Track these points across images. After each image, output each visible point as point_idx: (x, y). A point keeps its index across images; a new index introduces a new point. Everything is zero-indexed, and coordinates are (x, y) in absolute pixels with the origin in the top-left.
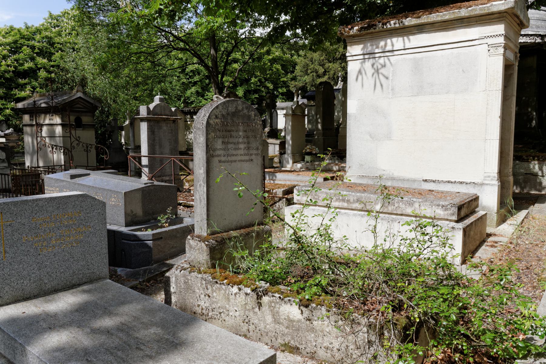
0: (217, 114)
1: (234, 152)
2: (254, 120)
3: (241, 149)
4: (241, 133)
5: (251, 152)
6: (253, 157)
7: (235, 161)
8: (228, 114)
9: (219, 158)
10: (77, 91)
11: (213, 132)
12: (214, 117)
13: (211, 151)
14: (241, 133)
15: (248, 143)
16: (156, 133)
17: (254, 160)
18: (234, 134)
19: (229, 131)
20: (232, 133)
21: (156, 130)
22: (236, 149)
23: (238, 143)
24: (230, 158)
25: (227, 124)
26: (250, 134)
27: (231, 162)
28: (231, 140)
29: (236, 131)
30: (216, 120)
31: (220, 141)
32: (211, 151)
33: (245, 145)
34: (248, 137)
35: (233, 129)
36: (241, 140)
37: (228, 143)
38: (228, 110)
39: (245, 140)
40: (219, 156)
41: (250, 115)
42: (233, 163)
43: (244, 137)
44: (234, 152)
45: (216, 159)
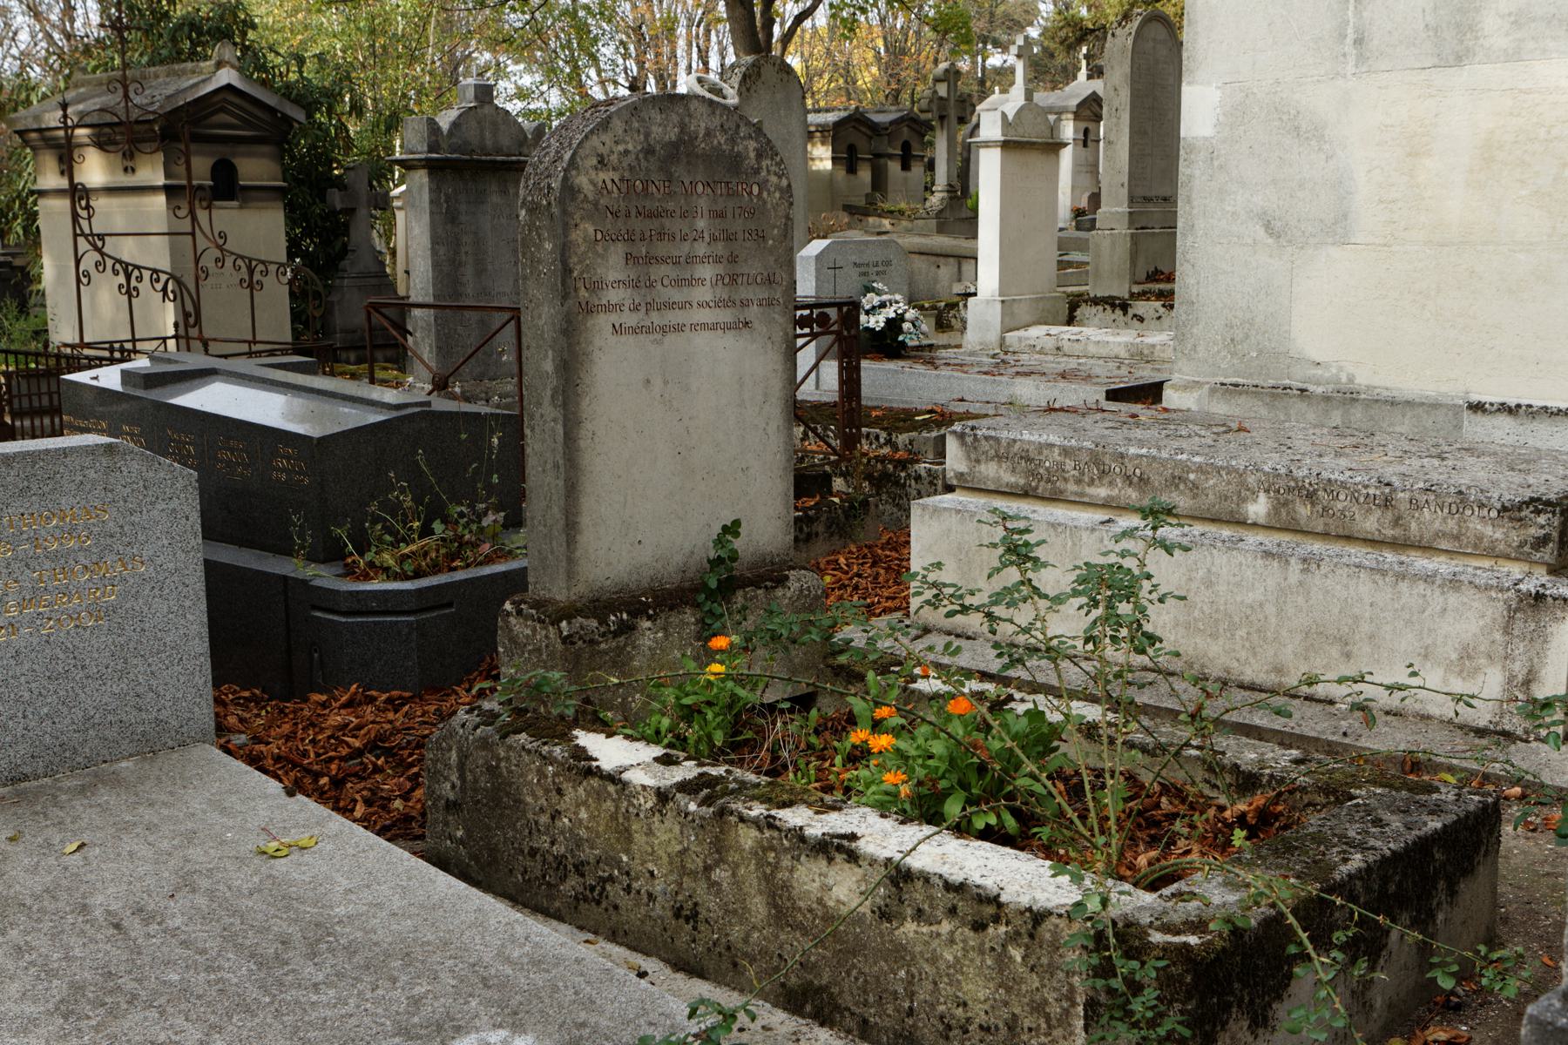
0: (601, 149)
1: (676, 295)
2: (757, 171)
3: (702, 281)
4: (701, 224)
5: (745, 293)
6: (753, 312)
7: (679, 328)
8: (649, 151)
9: (614, 318)
10: (219, 65)
11: (589, 217)
12: (594, 162)
13: (583, 293)
14: (701, 224)
15: (733, 259)
16: (463, 218)
17: (756, 324)
18: (674, 225)
19: (651, 215)
20: (667, 222)
21: (463, 207)
22: (679, 283)
23: (691, 260)
24: (656, 318)
25: (645, 189)
26: (738, 226)
27: (664, 330)
28: (662, 249)
29: (683, 216)
30: (602, 176)
31: (617, 253)
32: (583, 293)
33: (720, 269)
34: (730, 238)
35: (671, 206)
36: (701, 249)
37: (651, 260)
38: (647, 135)
39: (720, 249)
40: (610, 308)
41: (739, 154)
42: (671, 338)
43: (714, 239)
44: (676, 295)
45: (603, 321)
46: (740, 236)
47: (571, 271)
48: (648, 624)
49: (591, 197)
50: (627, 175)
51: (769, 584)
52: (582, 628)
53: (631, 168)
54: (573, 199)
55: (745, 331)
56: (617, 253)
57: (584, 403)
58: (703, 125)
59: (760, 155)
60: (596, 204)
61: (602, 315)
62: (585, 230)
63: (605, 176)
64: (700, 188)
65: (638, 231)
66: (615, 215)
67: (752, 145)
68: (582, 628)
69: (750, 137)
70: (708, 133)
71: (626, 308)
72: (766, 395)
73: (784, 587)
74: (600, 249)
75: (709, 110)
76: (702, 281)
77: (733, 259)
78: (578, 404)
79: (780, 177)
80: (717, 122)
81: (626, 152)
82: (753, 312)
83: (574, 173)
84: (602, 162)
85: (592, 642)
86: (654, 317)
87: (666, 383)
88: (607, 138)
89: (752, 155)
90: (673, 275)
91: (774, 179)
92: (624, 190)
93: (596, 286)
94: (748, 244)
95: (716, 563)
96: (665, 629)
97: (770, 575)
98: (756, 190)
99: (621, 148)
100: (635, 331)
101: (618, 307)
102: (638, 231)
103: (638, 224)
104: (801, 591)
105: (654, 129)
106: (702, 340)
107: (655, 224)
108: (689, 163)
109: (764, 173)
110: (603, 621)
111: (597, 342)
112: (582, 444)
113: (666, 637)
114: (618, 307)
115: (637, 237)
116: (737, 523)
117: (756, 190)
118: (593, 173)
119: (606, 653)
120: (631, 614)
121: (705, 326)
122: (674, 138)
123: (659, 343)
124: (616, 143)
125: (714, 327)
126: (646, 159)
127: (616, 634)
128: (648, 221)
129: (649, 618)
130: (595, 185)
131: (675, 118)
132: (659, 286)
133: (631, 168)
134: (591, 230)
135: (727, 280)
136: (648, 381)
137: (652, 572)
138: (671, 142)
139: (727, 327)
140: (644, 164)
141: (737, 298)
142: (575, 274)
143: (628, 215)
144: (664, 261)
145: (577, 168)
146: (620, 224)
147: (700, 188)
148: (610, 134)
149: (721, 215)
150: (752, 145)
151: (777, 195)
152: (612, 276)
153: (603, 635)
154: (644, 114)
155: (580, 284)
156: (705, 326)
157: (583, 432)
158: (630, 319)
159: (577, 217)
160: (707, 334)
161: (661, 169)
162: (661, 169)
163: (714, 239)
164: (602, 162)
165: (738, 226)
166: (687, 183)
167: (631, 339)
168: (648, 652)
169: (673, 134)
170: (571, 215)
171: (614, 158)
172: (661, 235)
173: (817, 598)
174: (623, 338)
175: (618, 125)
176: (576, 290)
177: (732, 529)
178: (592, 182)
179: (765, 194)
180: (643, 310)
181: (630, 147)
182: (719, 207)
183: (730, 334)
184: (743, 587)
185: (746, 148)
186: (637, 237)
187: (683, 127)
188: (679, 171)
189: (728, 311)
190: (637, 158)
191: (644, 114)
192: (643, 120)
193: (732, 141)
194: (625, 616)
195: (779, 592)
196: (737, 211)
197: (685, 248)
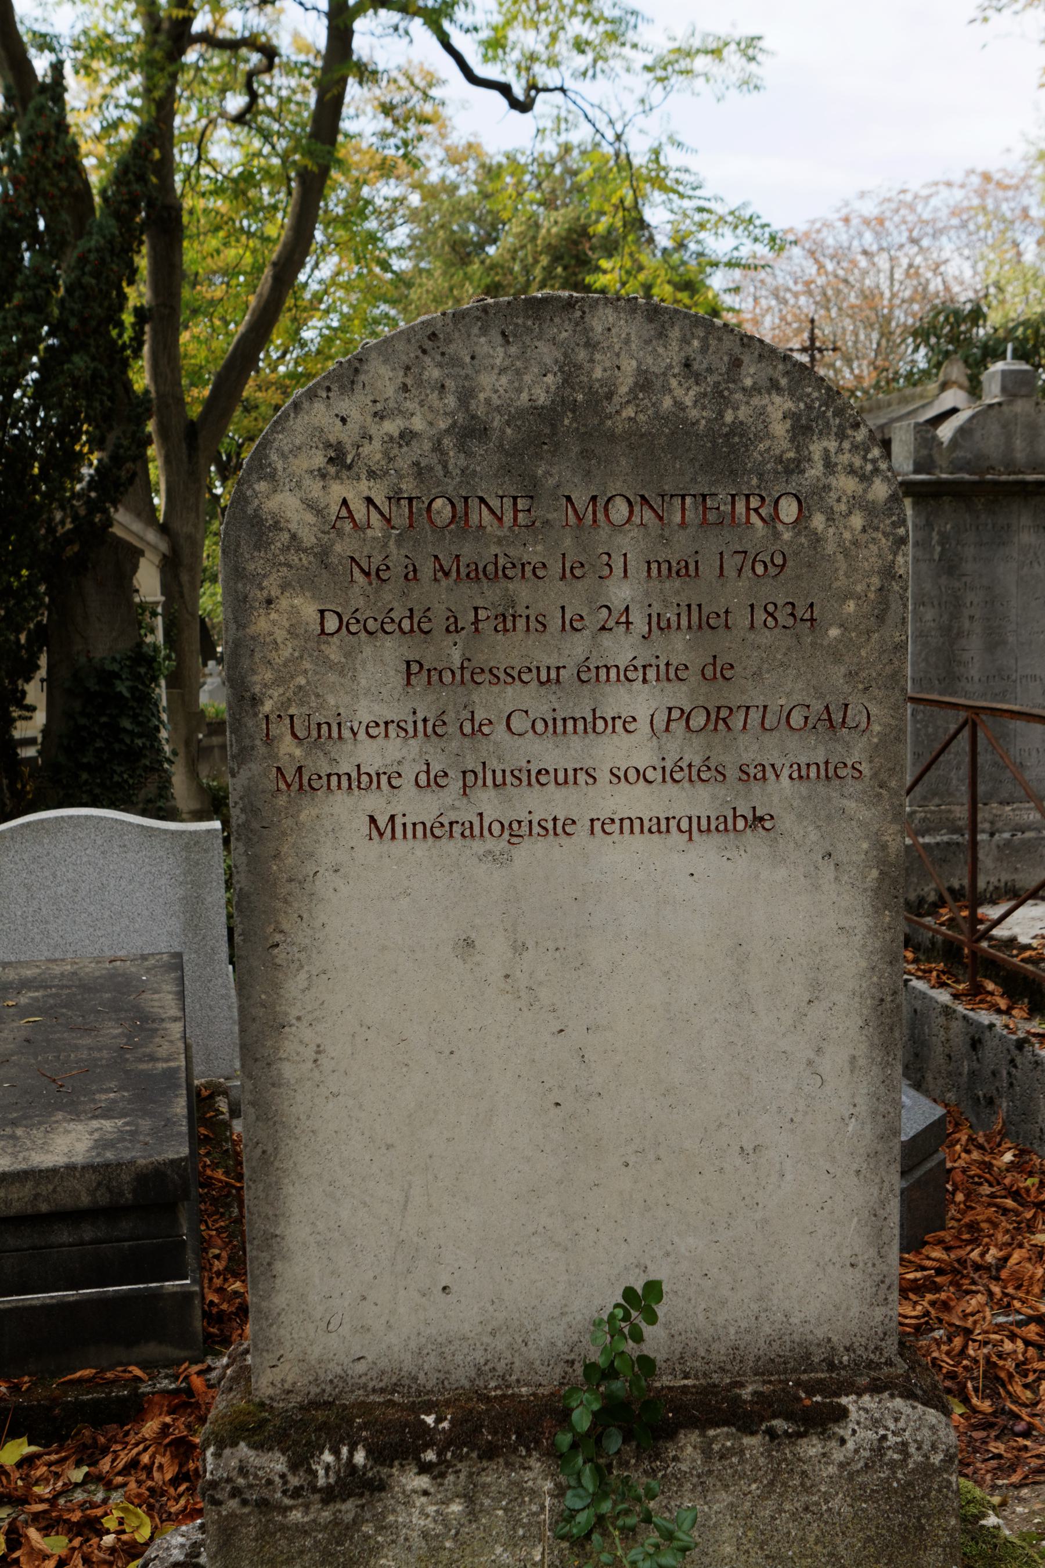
0: (336, 432)
1: (549, 754)
2: (794, 467)
3: (628, 724)
4: (621, 593)
5: (749, 750)
6: (779, 794)
7: (558, 828)
8: (471, 431)
9: (375, 803)
11: (306, 583)
12: (319, 460)
13: (288, 748)
14: (621, 593)
15: (718, 672)
16: (969, 567)
17: (787, 822)
18: (547, 597)
19: (476, 574)
20: (523, 592)
22: (556, 726)
23: (591, 674)
24: (489, 803)
25: (460, 518)
26: (735, 594)
27: (513, 831)
28: (507, 650)
29: (570, 574)
30: (338, 490)
31: (380, 663)
32: (288, 748)
33: (679, 695)
34: (706, 623)
35: (533, 552)
36: (621, 649)
37: (471, 674)
38: (466, 396)
39: (678, 647)
40: (359, 781)
41: (738, 428)
42: (531, 852)
43: (659, 625)
44: (549, 754)
45: (345, 812)
46: (741, 619)
47: (256, 701)
48: (423, 1482)
49: (308, 538)
50: (408, 487)
51: (779, 1424)
52: (243, 1471)
53: (420, 471)
54: (261, 543)
55: (753, 839)
56: (380, 663)
57: (294, 985)
58: (629, 366)
59: (801, 429)
60: (323, 555)
61: (340, 796)
62: (294, 611)
63: (352, 490)
64: (620, 510)
65: (439, 613)
66: (376, 575)
67: (779, 405)
68: (243, 1471)
69: (774, 386)
70: (645, 383)
71: (406, 782)
72: (815, 986)
73: (825, 1435)
74: (333, 651)
75: (649, 330)
76: (628, 724)
77: (718, 672)
78: (276, 986)
79: (865, 478)
80: (671, 354)
81: (407, 436)
82: (779, 794)
83: (262, 486)
84: (339, 460)
85: (263, 1504)
86: (480, 796)
87: (519, 948)
88: (350, 406)
89: (780, 429)
90: (541, 708)
91: (848, 484)
92: (400, 519)
93: (324, 734)
94: (765, 638)
95: (599, 1374)
96: (469, 1499)
97: (788, 1397)
98: (789, 510)
99: (391, 427)
100: (429, 832)
101: (385, 779)
102: (439, 613)
103: (439, 598)
104: (879, 1449)
105: (486, 380)
106: (621, 854)
107: (491, 594)
108: (585, 454)
109: (815, 471)
110: (299, 1463)
111: (327, 854)
112: (288, 1071)
113: (472, 1514)
114: (385, 779)
115: (439, 623)
116: (654, 1289)
117: (789, 510)
118: (314, 488)
119: (303, 1531)
120: (379, 1455)
121: (631, 825)
122: (542, 399)
123: (501, 860)
124: (380, 416)
125: (661, 826)
126: (462, 447)
127: (329, 1495)
128: (467, 589)
129: (424, 1468)
130: (319, 512)
131: (547, 353)
132: (500, 731)
133: (420, 471)
134: (309, 611)
135: (698, 720)
136: (469, 943)
137: (479, 1356)
138: (536, 411)
139: (696, 828)
140: (456, 460)
141: (731, 764)
142: (267, 707)
143: (412, 575)
144: (515, 677)
145: (272, 477)
146: (389, 595)
147: (620, 510)
148: (361, 398)
149: (685, 571)
150: (779, 405)
151: (857, 521)
152: (365, 712)
153: (297, 1493)
154: (458, 348)
155: (282, 729)
156: (631, 825)
157: (289, 1047)
158: (416, 806)
159: (272, 585)
160: (639, 841)
161: (506, 470)
162: (506, 470)
163: (659, 625)
164: (339, 460)
165: (735, 594)
166: (581, 499)
167: (421, 849)
168: (417, 1541)
169: (540, 389)
170: (258, 581)
171: (373, 452)
172: (505, 620)
173: (926, 1470)
174: (400, 847)
175: (383, 378)
176: (269, 740)
177: (642, 1300)
178: (310, 505)
179: (818, 521)
180: (455, 785)
181: (418, 424)
182: (680, 547)
183: (707, 848)
184: (702, 1424)
185: (761, 413)
186: (439, 623)
187: (569, 372)
188: (558, 473)
189: (703, 792)
190: (438, 447)
191: (458, 348)
192: (455, 362)
193: (720, 398)
194: (360, 1457)
195: (811, 1448)
196: (731, 563)
197: (577, 647)
